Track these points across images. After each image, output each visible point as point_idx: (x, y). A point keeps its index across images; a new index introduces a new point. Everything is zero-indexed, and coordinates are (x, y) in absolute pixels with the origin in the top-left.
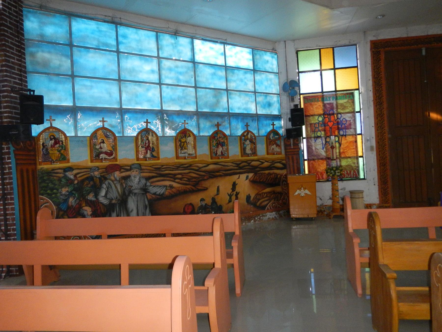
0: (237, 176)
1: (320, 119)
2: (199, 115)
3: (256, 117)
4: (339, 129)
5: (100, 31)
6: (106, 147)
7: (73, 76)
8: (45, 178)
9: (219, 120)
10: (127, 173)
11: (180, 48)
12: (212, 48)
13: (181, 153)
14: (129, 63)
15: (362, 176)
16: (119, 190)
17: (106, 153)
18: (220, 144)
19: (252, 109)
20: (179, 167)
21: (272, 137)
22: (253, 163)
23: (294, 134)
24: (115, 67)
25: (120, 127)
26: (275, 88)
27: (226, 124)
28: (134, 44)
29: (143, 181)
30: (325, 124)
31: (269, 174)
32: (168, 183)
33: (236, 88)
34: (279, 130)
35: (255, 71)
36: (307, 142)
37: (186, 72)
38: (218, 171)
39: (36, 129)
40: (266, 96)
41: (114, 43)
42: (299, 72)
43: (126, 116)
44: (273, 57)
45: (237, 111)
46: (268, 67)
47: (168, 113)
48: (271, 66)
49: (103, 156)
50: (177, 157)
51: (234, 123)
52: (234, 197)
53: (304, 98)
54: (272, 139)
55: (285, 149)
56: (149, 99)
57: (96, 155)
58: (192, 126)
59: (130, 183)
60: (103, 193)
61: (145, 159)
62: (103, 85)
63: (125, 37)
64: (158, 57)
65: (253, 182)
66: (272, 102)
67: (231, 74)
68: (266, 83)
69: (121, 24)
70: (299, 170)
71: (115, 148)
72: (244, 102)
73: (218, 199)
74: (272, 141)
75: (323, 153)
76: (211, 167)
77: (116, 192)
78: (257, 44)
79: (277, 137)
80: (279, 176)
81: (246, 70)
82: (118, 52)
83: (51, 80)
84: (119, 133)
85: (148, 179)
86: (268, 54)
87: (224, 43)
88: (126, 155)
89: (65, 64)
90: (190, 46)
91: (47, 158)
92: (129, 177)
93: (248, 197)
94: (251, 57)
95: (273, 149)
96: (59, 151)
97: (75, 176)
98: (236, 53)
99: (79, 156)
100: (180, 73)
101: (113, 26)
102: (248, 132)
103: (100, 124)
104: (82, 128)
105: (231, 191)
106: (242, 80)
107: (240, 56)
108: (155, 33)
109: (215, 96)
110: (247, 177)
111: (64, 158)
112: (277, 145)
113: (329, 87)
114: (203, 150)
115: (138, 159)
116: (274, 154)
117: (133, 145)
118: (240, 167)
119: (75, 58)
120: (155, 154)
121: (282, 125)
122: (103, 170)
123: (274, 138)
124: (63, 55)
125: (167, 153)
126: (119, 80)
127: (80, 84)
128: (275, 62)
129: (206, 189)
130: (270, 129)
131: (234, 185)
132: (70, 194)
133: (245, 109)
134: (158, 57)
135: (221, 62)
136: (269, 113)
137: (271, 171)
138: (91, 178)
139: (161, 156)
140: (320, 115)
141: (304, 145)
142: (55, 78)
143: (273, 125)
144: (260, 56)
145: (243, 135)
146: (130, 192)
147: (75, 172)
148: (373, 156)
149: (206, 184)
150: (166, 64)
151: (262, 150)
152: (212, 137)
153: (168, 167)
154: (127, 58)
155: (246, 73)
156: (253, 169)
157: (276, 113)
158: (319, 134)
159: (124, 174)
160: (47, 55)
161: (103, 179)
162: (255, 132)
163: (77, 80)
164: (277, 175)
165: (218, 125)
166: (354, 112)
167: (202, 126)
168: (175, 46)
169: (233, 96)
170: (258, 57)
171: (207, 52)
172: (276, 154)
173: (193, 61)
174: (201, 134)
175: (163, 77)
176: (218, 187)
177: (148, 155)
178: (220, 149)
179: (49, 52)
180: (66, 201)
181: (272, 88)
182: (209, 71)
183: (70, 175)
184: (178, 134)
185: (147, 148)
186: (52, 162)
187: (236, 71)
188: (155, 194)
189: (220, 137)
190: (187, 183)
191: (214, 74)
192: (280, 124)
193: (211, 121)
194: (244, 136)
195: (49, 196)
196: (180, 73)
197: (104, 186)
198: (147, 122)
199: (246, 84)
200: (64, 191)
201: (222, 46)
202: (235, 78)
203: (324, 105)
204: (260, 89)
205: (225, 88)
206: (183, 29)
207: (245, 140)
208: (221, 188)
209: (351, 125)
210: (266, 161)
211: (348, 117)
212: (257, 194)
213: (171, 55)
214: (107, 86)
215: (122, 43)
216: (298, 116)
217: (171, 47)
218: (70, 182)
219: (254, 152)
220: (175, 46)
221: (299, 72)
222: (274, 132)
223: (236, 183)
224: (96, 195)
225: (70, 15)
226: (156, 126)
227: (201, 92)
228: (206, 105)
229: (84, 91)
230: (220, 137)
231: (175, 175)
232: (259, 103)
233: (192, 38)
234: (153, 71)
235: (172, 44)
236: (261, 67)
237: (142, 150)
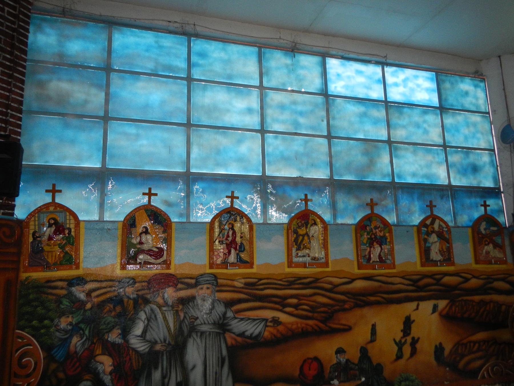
0: (414, 305)
2: (334, 185)
3: (449, 191)
5: (160, 47)
7: (106, 119)
8: (31, 297)
9: (375, 196)
11: (301, 72)
12: (359, 72)
13: (297, 256)
14: (209, 98)
16: (171, 325)
17: (149, 252)
18: (376, 240)
19: (441, 176)
20: (293, 282)
21: (485, 229)
22: (447, 279)
24: (182, 104)
27: (389, 203)
28: (218, 67)
29: (220, 309)
31: (482, 303)
32: (269, 314)
33: (406, 139)
34: (498, 216)
35: (442, 109)
37: (312, 112)
38: (374, 293)
40: (467, 154)
41: (184, 65)
43: (197, 187)
44: (476, 86)
45: (410, 180)
46: (468, 102)
47: (275, 181)
48: (474, 101)
50: (290, 264)
51: (404, 201)
52: (407, 350)
54: (484, 232)
56: (241, 157)
58: (320, 205)
59: (193, 312)
60: (138, 330)
61: (225, 264)
62: (159, 134)
63: (202, 55)
64: (261, 87)
65: (448, 318)
66: (480, 163)
67: (397, 115)
68: (465, 131)
69: (198, 36)
72: (423, 163)
73: (373, 352)
74: (484, 236)
76: (359, 284)
78: (444, 64)
79: (495, 229)
80: (504, 307)
81: (426, 108)
82: (189, 79)
83: (67, 126)
84: (181, 215)
85: (229, 304)
86: (467, 80)
87: (383, 64)
89: (96, 99)
92: (192, 299)
93: (439, 350)
94: (434, 86)
95: (488, 253)
96: (62, 247)
97: (89, 294)
98: (405, 80)
99: (100, 257)
100: (301, 114)
101: (184, 39)
102: (434, 218)
104: (113, 207)
105: (401, 334)
107: (415, 86)
108: (256, 49)
109: (366, 153)
110: (435, 308)
111: (70, 260)
112: (496, 246)
114: (343, 253)
116: (490, 263)
117: (204, 239)
118: (419, 287)
119: (112, 89)
122: (144, 284)
123: (488, 232)
124: (93, 85)
125: (270, 255)
128: (481, 94)
129: (348, 329)
131: (408, 323)
132: (75, 329)
133: (427, 176)
134: (261, 87)
135: (377, 93)
136: (475, 183)
137: (487, 298)
138: (118, 301)
139: (257, 261)
142: (75, 122)
143: (485, 206)
144: (452, 84)
145: (423, 223)
146: (193, 329)
150: (274, 98)
151: (464, 254)
152: (361, 227)
153: (269, 281)
154: (205, 88)
155: (425, 113)
157: (489, 183)
160: (65, 86)
161: (142, 301)
162: (448, 219)
163: (113, 125)
165: (372, 205)
167: (341, 205)
168: (292, 69)
169: (402, 153)
170: (447, 85)
172: (496, 263)
173: (325, 93)
174: (339, 221)
175: (269, 120)
176: (374, 326)
177: (232, 258)
178: (377, 250)
179: (71, 81)
180: (65, 342)
181: (478, 139)
182: (353, 109)
184: (291, 220)
185: (231, 245)
186: (48, 267)
187: (405, 110)
188: (242, 335)
189: (376, 228)
190: (310, 314)
191: (364, 115)
192: (497, 204)
193: (357, 197)
194: (426, 226)
195: (36, 332)
196: (301, 114)
197: (143, 316)
198: (232, 197)
199: (426, 132)
200: (64, 323)
201: (378, 70)
202: (404, 121)
204: (453, 140)
205: (385, 137)
206: (304, 40)
207: (428, 234)
210: (474, 277)
212: (457, 344)
213: (284, 84)
214: (166, 135)
215: (197, 65)
217: (285, 71)
219: (448, 257)
220: (292, 69)
222: (488, 219)
223: (412, 318)
224: (125, 333)
225: (111, 24)
226: (250, 204)
227: (339, 146)
228: (348, 167)
230: (376, 228)
231: (286, 297)
232: (454, 165)
233: (324, 55)
234: (250, 111)
235: (287, 66)
236: (455, 103)
237: (220, 248)
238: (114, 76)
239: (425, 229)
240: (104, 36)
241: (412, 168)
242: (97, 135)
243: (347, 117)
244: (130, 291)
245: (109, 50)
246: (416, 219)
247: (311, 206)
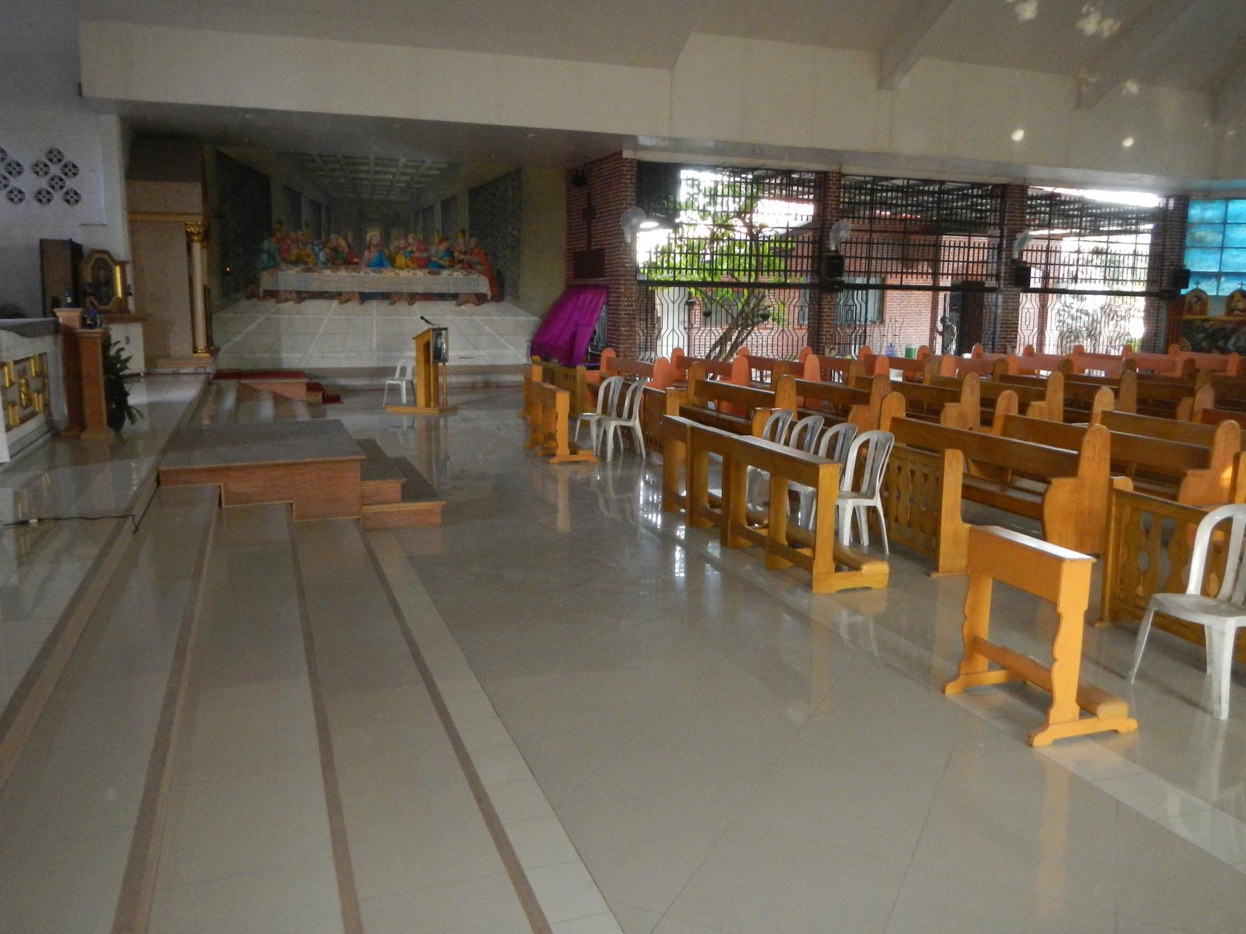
7: (1222, 248)
39: (1183, 292)
57: (1230, 311)
60: (1232, 342)
91: (1190, 310)
99: (1217, 312)
132: (1204, 339)
138: (1223, 329)
161: (1234, 330)
183: (1207, 325)
200: (1200, 336)
218: (1205, 330)
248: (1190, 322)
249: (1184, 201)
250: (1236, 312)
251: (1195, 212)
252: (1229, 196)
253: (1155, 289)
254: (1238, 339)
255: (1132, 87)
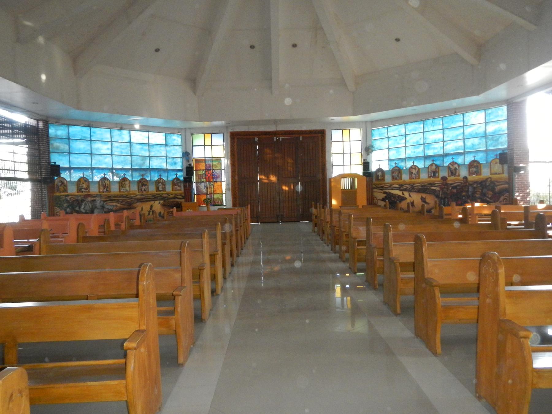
1: (204, 172)
2: (133, 170)
3: (167, 171)
4: (213, 178)
6: (85, 186)
7: (69, 153)
10: (94, 198)
11: (123, 136)
14: (96, 145)
15: (224, 204)
17: (84, 189)
18: (143, 185)
19: (164, 167)
22: (164, 195)
23: (188, 180)
25: (91, 176)
26: (180, 154)
27: (148, 174)
28: (99, 136)
29: (102, 203)
30: (206, 175)
32: (115, 204)
35: (166, 145)
36: (196, 184)
42: (193, 146)
43: (94, 171)
46: (175, 143)
49: (83, 190)
50: (120, 191)
51: (153, 174)
52: (151, 213)
53: (196, 160)
55: (184, 188)
56: (106, 162)
57: (79, 190)
58: (128, 176)
60: (83, 207)
61: (103, 192)
63: (94, 133)
64: (111, 142)
65: (163, 205)
66: (177, 162)
70: (191, 199)
71: (88, 186)
75: (204, 191)
76: (138, 197)
77: (89, 206)
78: (167, 131)
82: (91, 140)
83: (60, 155)
85: (104, 201)
86: (175, 135)
87: (148, 131)
88: (94, 190)
89: (66, 147)
90: (128, 135)
92: (95, 200)
99: (72, 190)
100: (123, 149)
101: (89, 128)
102: (161, 179)
103: (82, 175)
106: (158, 151)
107: (158, 138)
109: (142, 160)
110: (159, 203)
111: (65, 190)
112: (179, 186)
113: (208, 155)
114: (134, 188)
115: (100, 192)
117: (97, 185)
118: (155, 198)
120: (108, 189)
121: (181, 176)
125: (115, 189)
126: (91, 154)
127: (73, 157)
129: (135, 208)
130: (175, 177)
131: (152, 206)
132: (68, 207)
133: (160, 166)
134: (111, 142)
138: (77, 200)
139: (112, 191)
140: (203, 170)
141: (195, 185)
145: (157, 180)
146: (96, 207)
147: (70, 197)
148: (230, 193)
149: (135, 205)
150: (115, 144)
151: (169, 188)
153: (115, 196)
156: (163, 198)
157: (179, 168)
158: (203, 180)
159: (92, 199)
161: (83, 201)
162: (165, 179)
163: (71, 154)
164: (178, 202)
165: (143, 175)
166: (221, 169)
167: (134, 175)
168: (120, 135)
170: (168, 137)
171: (138, 137)
173: (130, 142)
175: (113, 151)
177: (105, 190)
178: (144, 188)
182: (138, 147)
183: (68, 198)
184: (121, 180)
185: (105, 187)
187: (155, 146)
191: (142, 148)
195: (59, 207)
196: (123, 149)
198: (105, 174)
199: (161, 153)
200: (65, 205)
201: (147, 133)
203: (206, 165)
204: (168, 155)
206: (124, 127)
208: (144, 208)
209: (219, 176)
211: (218, 172)
216: (189, 170)
218: (68, 201)
219: (164, 189)
220: (120, 135)
221: (193, 146)
222: (177, 179)
224: (80, 208)
226: (109, 176)
227: (134, 158)
228: (136, 165)
229: (74, 159)
231: (118, 200)
234: (108, 149)
237: (102, 188)
238: (70, 140)
239: (157, 182)
240: (67, 129)
241: (156, 164)
242: (68, 158)
243: (137, 149)
244: (80, 198)
245: (69, 134)
246: (156, 179)
247: (126, 176)
248: (59, 197)
249: (46, 123)
250: (83, 190)
251: (52, 131)
252: (70, 123)
253: (38, 177)
254: (85, 204)
255: (41, 40)
